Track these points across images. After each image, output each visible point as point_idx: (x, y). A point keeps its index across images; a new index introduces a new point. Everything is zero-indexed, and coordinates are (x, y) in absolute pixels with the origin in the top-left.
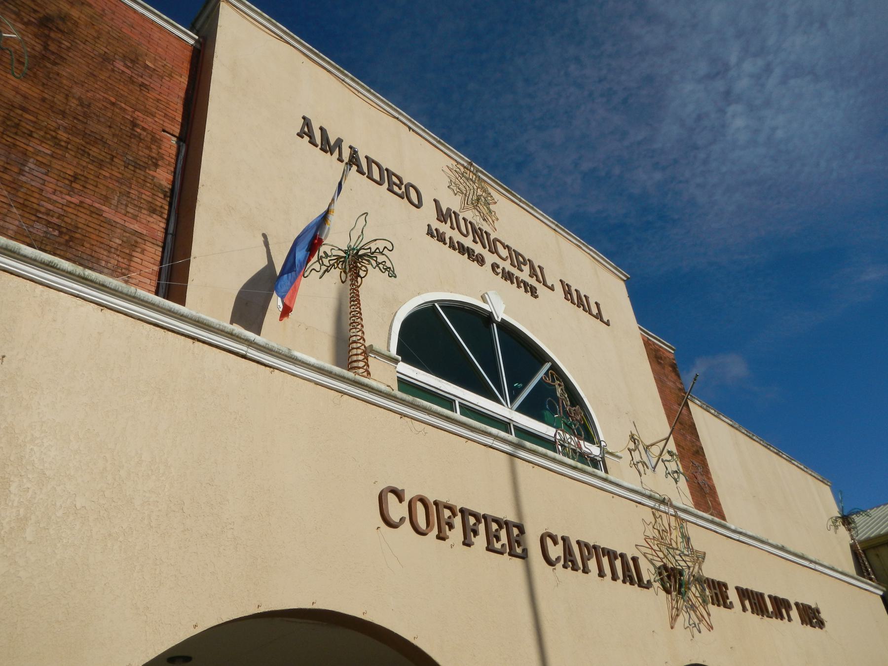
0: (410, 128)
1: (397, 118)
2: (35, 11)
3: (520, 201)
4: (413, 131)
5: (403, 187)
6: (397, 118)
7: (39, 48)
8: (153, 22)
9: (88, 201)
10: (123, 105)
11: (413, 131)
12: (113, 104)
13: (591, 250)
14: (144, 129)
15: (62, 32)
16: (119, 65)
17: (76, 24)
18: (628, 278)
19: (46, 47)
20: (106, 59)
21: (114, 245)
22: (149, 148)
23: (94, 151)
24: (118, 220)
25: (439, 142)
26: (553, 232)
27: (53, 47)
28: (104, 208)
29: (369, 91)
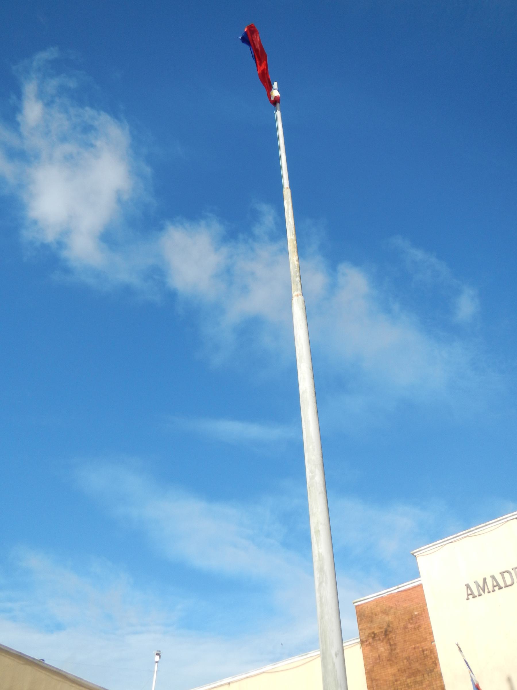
1: (508, 521)
2: (382, 632)
6: (508, 521)
7: (389, 647)
10: (417, 645)
12: (414, 648)
14: (427, 650)
15: (390, 632)
16: (410, 626)
17: (392, 623)
19: (390, 645)
20: (405, 628)
22: (431, 658)
23: (419, 678)
27: (392, 643)
29: (486, 525)
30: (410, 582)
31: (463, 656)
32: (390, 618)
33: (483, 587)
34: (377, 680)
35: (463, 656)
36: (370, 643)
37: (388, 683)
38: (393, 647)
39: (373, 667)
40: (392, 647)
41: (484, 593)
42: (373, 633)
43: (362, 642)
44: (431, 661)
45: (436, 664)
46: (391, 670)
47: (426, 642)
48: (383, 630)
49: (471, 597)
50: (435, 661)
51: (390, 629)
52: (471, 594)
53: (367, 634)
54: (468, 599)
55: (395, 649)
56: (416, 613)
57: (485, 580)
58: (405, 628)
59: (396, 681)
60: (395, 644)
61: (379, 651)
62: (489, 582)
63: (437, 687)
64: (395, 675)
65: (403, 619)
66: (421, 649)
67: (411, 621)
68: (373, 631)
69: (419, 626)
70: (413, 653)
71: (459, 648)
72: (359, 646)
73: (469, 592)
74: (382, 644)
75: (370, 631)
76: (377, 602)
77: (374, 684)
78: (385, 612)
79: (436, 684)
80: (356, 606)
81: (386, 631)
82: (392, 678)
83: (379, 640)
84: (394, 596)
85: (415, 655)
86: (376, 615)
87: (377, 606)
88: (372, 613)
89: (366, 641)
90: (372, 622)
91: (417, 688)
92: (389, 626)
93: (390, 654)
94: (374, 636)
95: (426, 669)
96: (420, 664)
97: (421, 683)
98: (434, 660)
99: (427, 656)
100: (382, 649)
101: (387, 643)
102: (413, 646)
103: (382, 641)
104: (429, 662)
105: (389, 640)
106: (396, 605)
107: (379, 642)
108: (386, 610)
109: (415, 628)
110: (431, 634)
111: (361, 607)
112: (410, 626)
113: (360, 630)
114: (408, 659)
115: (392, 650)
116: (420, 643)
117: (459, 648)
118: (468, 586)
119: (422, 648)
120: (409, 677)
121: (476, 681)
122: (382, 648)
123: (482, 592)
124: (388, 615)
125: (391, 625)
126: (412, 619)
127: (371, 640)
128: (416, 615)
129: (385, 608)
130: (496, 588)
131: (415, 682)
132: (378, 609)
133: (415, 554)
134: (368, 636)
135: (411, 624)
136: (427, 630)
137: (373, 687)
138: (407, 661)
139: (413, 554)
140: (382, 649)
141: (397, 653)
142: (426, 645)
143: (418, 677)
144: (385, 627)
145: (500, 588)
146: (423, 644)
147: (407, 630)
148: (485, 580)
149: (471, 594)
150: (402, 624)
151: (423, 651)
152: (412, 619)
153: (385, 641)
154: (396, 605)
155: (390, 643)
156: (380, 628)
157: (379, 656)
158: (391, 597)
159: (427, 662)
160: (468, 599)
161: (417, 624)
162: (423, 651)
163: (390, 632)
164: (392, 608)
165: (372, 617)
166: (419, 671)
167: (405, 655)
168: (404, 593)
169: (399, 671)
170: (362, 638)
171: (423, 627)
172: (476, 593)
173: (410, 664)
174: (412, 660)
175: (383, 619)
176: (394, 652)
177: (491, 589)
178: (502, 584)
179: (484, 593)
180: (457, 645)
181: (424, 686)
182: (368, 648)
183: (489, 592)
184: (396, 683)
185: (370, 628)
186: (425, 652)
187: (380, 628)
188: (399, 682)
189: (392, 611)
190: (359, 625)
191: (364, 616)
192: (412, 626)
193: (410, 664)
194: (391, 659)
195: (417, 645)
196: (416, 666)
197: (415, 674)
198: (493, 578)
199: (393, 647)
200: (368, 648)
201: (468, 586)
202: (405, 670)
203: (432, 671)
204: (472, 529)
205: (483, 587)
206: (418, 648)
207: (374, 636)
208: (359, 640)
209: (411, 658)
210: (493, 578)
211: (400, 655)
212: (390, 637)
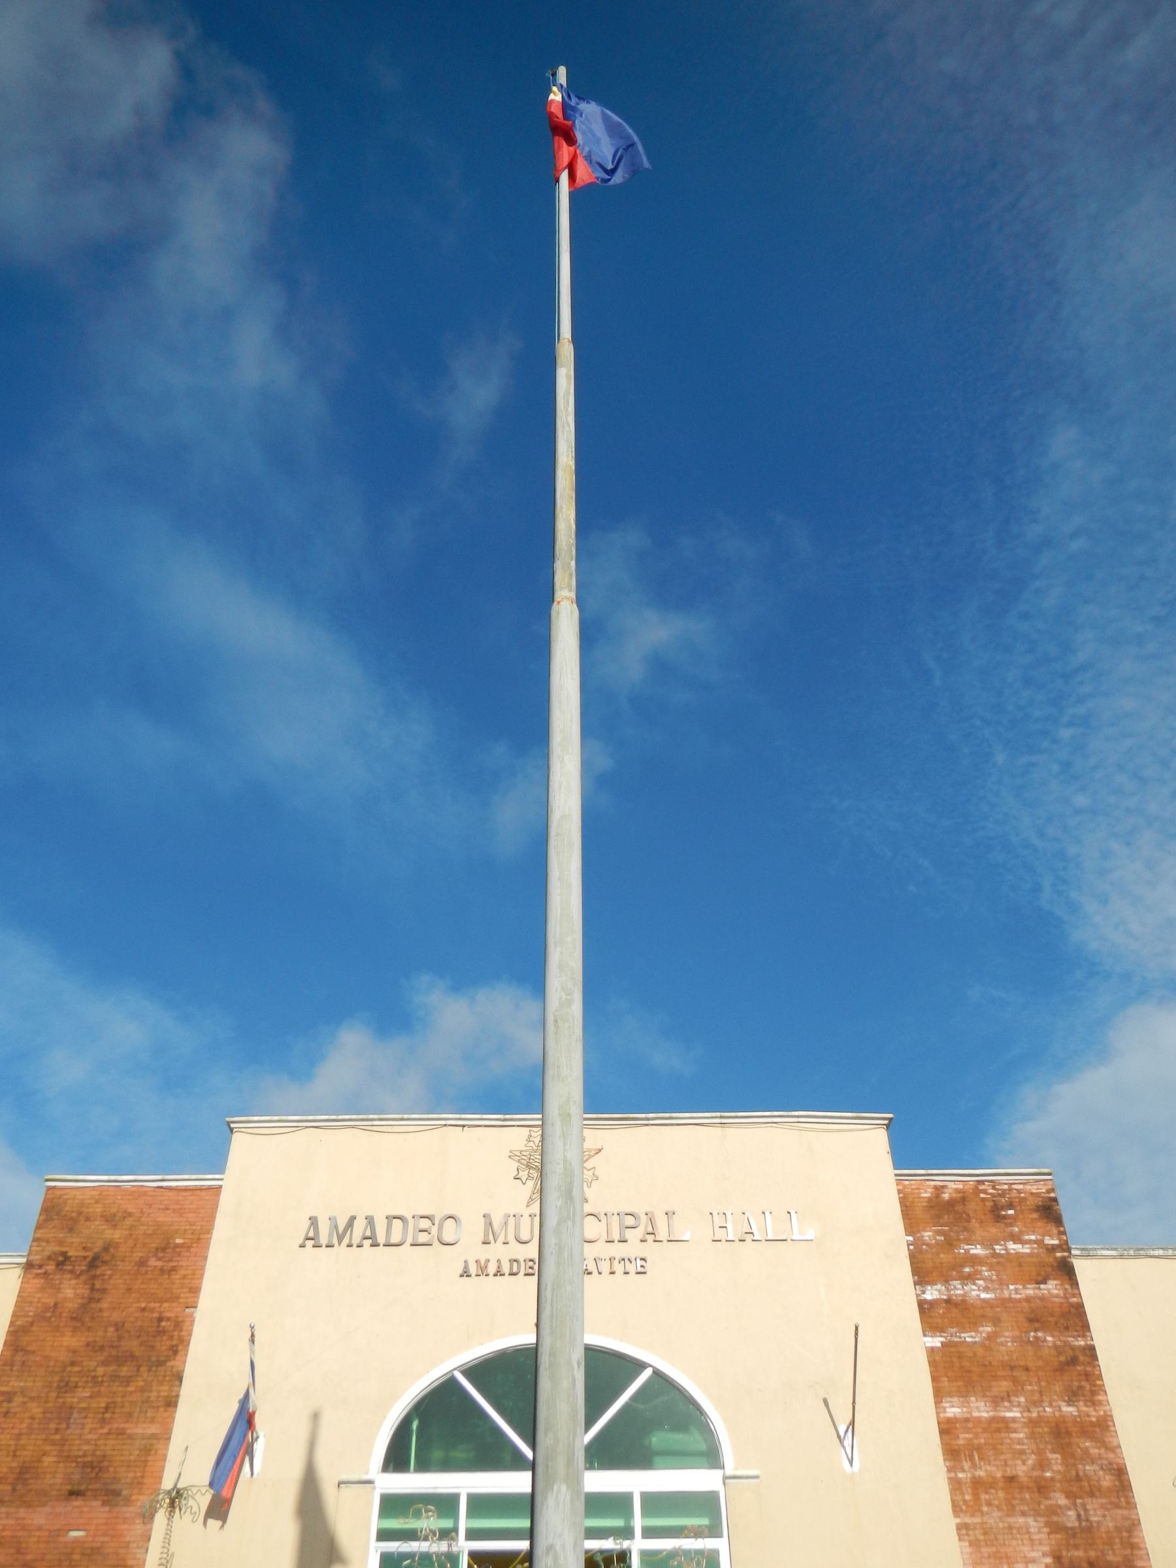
0: (464, 1126)
2: (85, 1258)
3: (648, 1119)
4: (470, 1126)
5: (434, 1230)
7: (86, 1293)
8: (186, 1189)
9: (115, 1426)
10: (152, 1305)
11: (470, 1126)
12: (144, 1310)
13: (798, 1117)
14: (168, 1319)
16: (153, 1262)
17: (117, 1246)
18: (890, 1119)
19: (92, 1289)
20: (142, 1263)
21: (132, 1458)
22: (171, 1338)
23: (125, 1371)
24: (139, 1431)
25: (505, 1120)
26: (718, 1131)
27: (97, 1286)
28: (127, 1425)
29: (402, 1119)
30: (194, 1177)
31: (252, 1352)
32: (116, 1235)
33: (342, 1233)
34: (27, 1352)
35: (252, 1352)
36: (45, 1273)
37: (51, 1364)
38: (97, 1296)
39: (32, 1324)
40: (95, 1294)
41: (340, 1244)
42: (64, 1254)
43: (29, 1266)
44: (168, 1343)
45: (176, 1352)
46: (71, 1340)
47: (174, 1305)
48: (90, 1254)
49: (310, 1243)
50: (176, 1346)
51: (107, 1258)
52: (312, 1239)
53: (47, 1253)
54: (303, 1246)
55: (99, 1300)
56: (178, 1241)
57: (353, 1218)
58: (142, 1263)
59: (73, 1364)
60: (104, 1291)
61: (60, 1295)
62: (359, 1228)
63: (158, 1397)
64: (74, 1352)
65: (144, 1245)
66: (156, 1315)
67: (161, 1255)
68: (64, 1249)
69: (174, 1269)
70: (137, 1318)
71: (253, 1335)
72: (18, 1272)
73: (311, 1234)
74: (73, 1282)
75: (57, 1249)
76: (101, 1194)
77: (19, 1358)
78: (111, 1220)
79: (159, 1391)
80: (49, 1188)
81: (96, 1258)
82: (64, 1357)
83: (72, 1272)
84: (145, 1194)
85: (139, 1323)
86: (88, 1219)
87: (97, 1202)
88: (80, 1213)
89: (40, 1267)
90: (71, 1230)
91: (114, 1389)
92: (106, 1249)
93: (83, 1306)
94: (62, 1261)
95: (149, 1357)
96: (141, 1344)
97: (128, 1381)
98: (175, 1342)
99: (161, 1332)
100: (69, 1293)
101: (85, 1283)
102: (143, 1305)
103: (78, 1277)
104: (163, 1344)
105: (94, 1277)
106: (142, 1212)
107: (69, 1276)
108: (115, 1215)
109: (162, 1271)
110: (195, 1291)
111: (59, 1192)
112: (153, 1262)
113: (35, 1240)
114: (118, 1326)
115: (91, 1300)
116: (161, 1301)
117: (253, 1335)
118: (314, 1221)
119: (161, 1313)
120: (105, 1363)
121: (254, 1406)
122: (71, 1291)
123: (335, 1241)
124: (115, 1227)
125: (111, 1250)
126: (164, 1249)
127: (51, 1267)
128: (177, 1246)
129: (114, 1210)
130: (367, 1243)
131: (115, 1377)
132: (99, 1209)
133: (232, 1125)
134: (49, 1258)
135: (159, 1259)
136: (187, 1281)
137: (12, 1365)
138: (117, 1330)
139: (228, 1123)
140: (69, 1293)
141: (101, 1310)
142: (170, 1310)
143: (125, 1368)
144: (96, 1250)
145: (375, 1245)
146: (166, 1305)
147: (143, 1269)
148: (353, 1218)
149: (312, 1239)
150: (137, 1255)
151: (160, 1319)
152: (164, 1249)
153: (84, 1277)
154: (142, 1212)
155: (93, 1285)
156: (84, 1248)
157: (56, 1305)
158: (139, 1193)
159: (158, 1344)
160: (303, 1246)
161: (171, 1264)
162: (160, 1319)
163: (105, 1262)
164: (130, 1215)
165: (75, 1221)
166: (132, 1357)
167: (116, 1317)
168: (171, 1193)
169: (88, 1345)
170: (31, 1258)
171: (183, 1272)
172: (324, 1240)
173: (120, 1338)
174: (128, 1332)
175: (99, 1233)
176: (93, 1305)
177: (356, 1240)
178: (381, 1239)
179: (340, 1244)
180: (252, 1328)
181: (131, 1389)
182: (38, 1282)
183: (350, 1246)
184: (69, 1369)
185: (61, 1243)
186: (163, 1324)
187: (84, 1248)
188: (76, 1369)
189: (129, 1221)
190: (39, 1227)
191: (58, 1214)
192: (159, 1264)
193: (120, 1338)
194: (80, 1318)
195: (152, 1305)
196: (132, 1345)
197: (119, 1360)
198: (370, 1220)
199: (97, 1296)
200: (36, 1281)
201: (314, 1221)
202: (102, 1348)
203: (160, 1363)
204: (371, 1116)
205: (342, 1233)
206: (152, 1310)
207: (62, 1261)
208: (24, 1260)
209: (127, 1326)
210: (370, 1220)
211: (105, 1314)
212: (98, 1272)
